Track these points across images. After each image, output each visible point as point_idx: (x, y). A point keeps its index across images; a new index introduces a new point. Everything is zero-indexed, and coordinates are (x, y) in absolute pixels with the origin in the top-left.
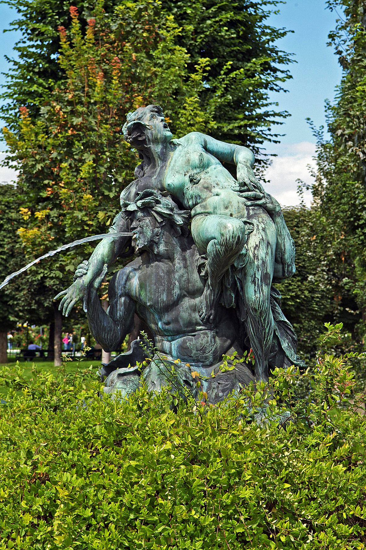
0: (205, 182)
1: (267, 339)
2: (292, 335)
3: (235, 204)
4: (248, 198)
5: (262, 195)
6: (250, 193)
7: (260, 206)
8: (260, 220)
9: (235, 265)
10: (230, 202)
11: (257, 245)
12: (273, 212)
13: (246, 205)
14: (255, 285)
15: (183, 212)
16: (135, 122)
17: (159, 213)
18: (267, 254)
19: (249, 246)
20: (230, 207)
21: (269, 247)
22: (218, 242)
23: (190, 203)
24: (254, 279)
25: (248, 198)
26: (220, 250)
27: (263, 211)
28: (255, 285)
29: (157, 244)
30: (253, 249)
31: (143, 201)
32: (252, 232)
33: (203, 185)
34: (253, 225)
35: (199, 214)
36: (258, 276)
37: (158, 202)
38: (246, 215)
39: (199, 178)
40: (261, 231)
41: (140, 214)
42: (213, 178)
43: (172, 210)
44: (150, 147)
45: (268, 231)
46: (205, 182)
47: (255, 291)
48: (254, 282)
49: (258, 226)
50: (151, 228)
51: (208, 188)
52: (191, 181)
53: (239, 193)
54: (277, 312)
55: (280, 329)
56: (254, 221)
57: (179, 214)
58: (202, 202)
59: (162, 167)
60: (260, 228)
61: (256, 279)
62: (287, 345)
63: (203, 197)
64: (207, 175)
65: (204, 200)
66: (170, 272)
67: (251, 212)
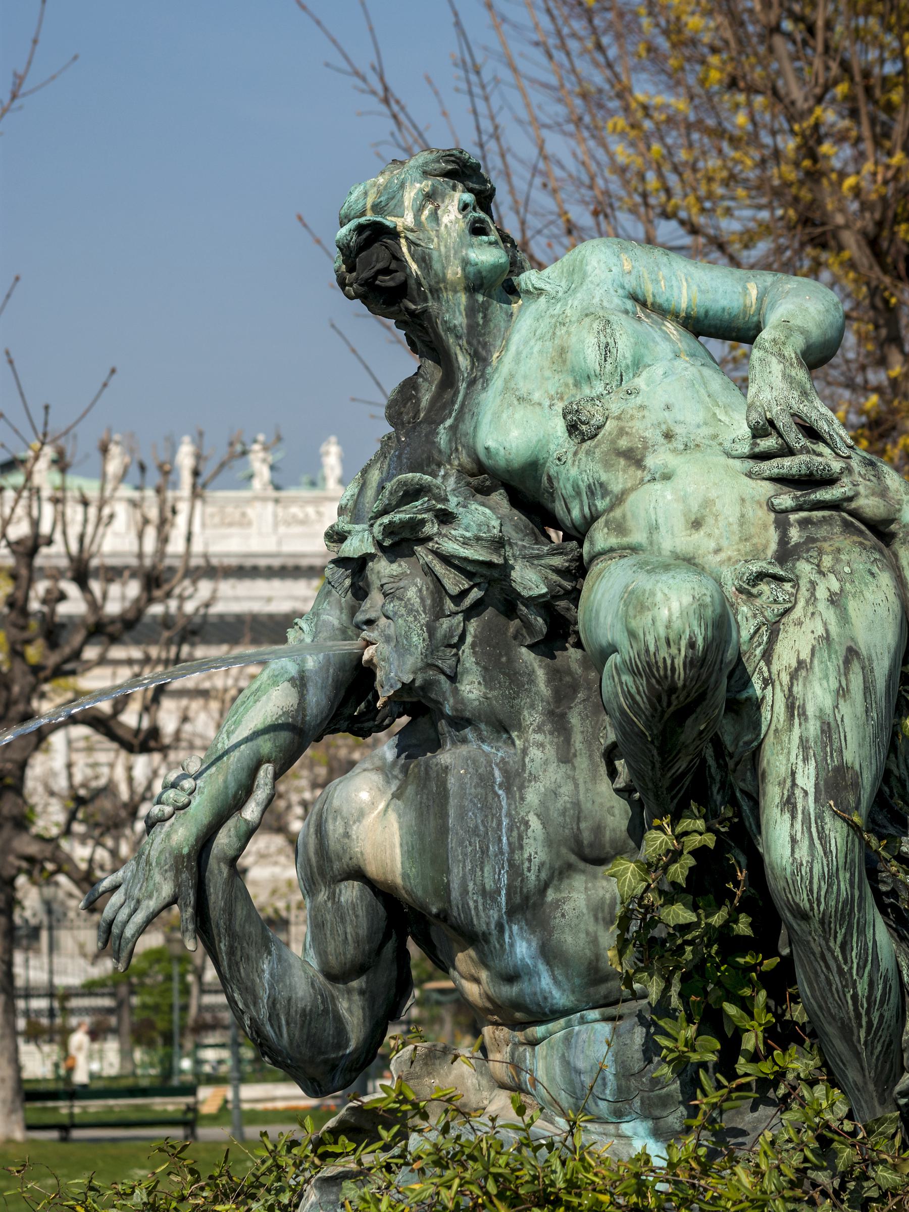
0: (622, 432)
1: (870, 1023)
3: (728, 511)
4: (781, 480)
5: (837, 466)
6: (787, 462)
7: (834, 506)
8: (827, 561)
9: (727, 739)
10: (707, 503)
11: (800, 663)
12: (893, 527)
13: (772, 508)
14: (793, 817)
16: (362, 220)
17: (447, 560)
18: (842, 692)
19: (775, 668)
20: (710, 520)
21: (856, 667)
22: (624, 662)
23: (576, 513)
24: (792, 794)
25: (781, 480)
26: (633, 691)
27: (847, 525)
28: (793, 817)
29: (453, 678)
30: (785, 678)
31: (386, 520)
32: (787, 611)
33: (613, 442)
34: (796, 586)
35: (601, 554)
36: (807, 779)
37: (445, 518)
38: (773, 547)
39: (598, 419)
40: (822, 606)
41: (383, 569)
42: (656, 414)
43: (499, 544)
44: (425, 311)
45: (852, 605)
46: (622, 432)
47: (794, 841)
48: (789, 804)
49: (813, 584)
50: (424, 618)
51: (634, 458)
52: (572, 428)
53: (750, 463)
56: (804, 568)
57: (531, 559)
58: (611, 508)
59: (472, 383)
60: (822, 593)
61: (798, 793)
63: (616, 487)
65: (620, 499)
66: (515, 779)
67: (795, 534)
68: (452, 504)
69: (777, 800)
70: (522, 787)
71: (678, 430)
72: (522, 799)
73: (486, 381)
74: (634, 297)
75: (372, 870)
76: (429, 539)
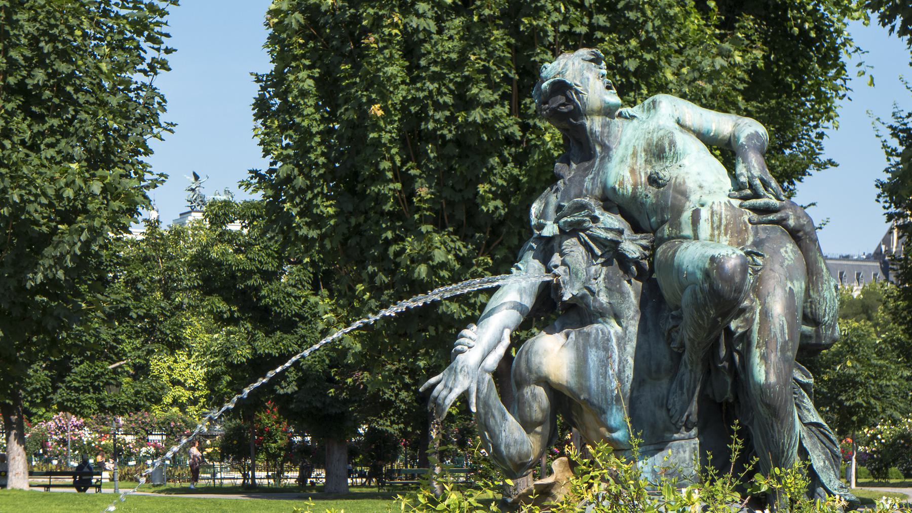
2: (831, 446)
15: (639, 236)
37: (595, 219)
43: (620, 232)
54: (805, 407)
55: (811, 437)
57: (633, 241)
59: (602, 159)
62: (822, 464)
64: (683, 170)
68: (597, 213)
69: (758, 354)
70: (625, 344)
71: (704, 184)
72: (625, 349)
73: (610, 158)
74: (678, 122)
75: (553, 378)
76: (588, 229)
